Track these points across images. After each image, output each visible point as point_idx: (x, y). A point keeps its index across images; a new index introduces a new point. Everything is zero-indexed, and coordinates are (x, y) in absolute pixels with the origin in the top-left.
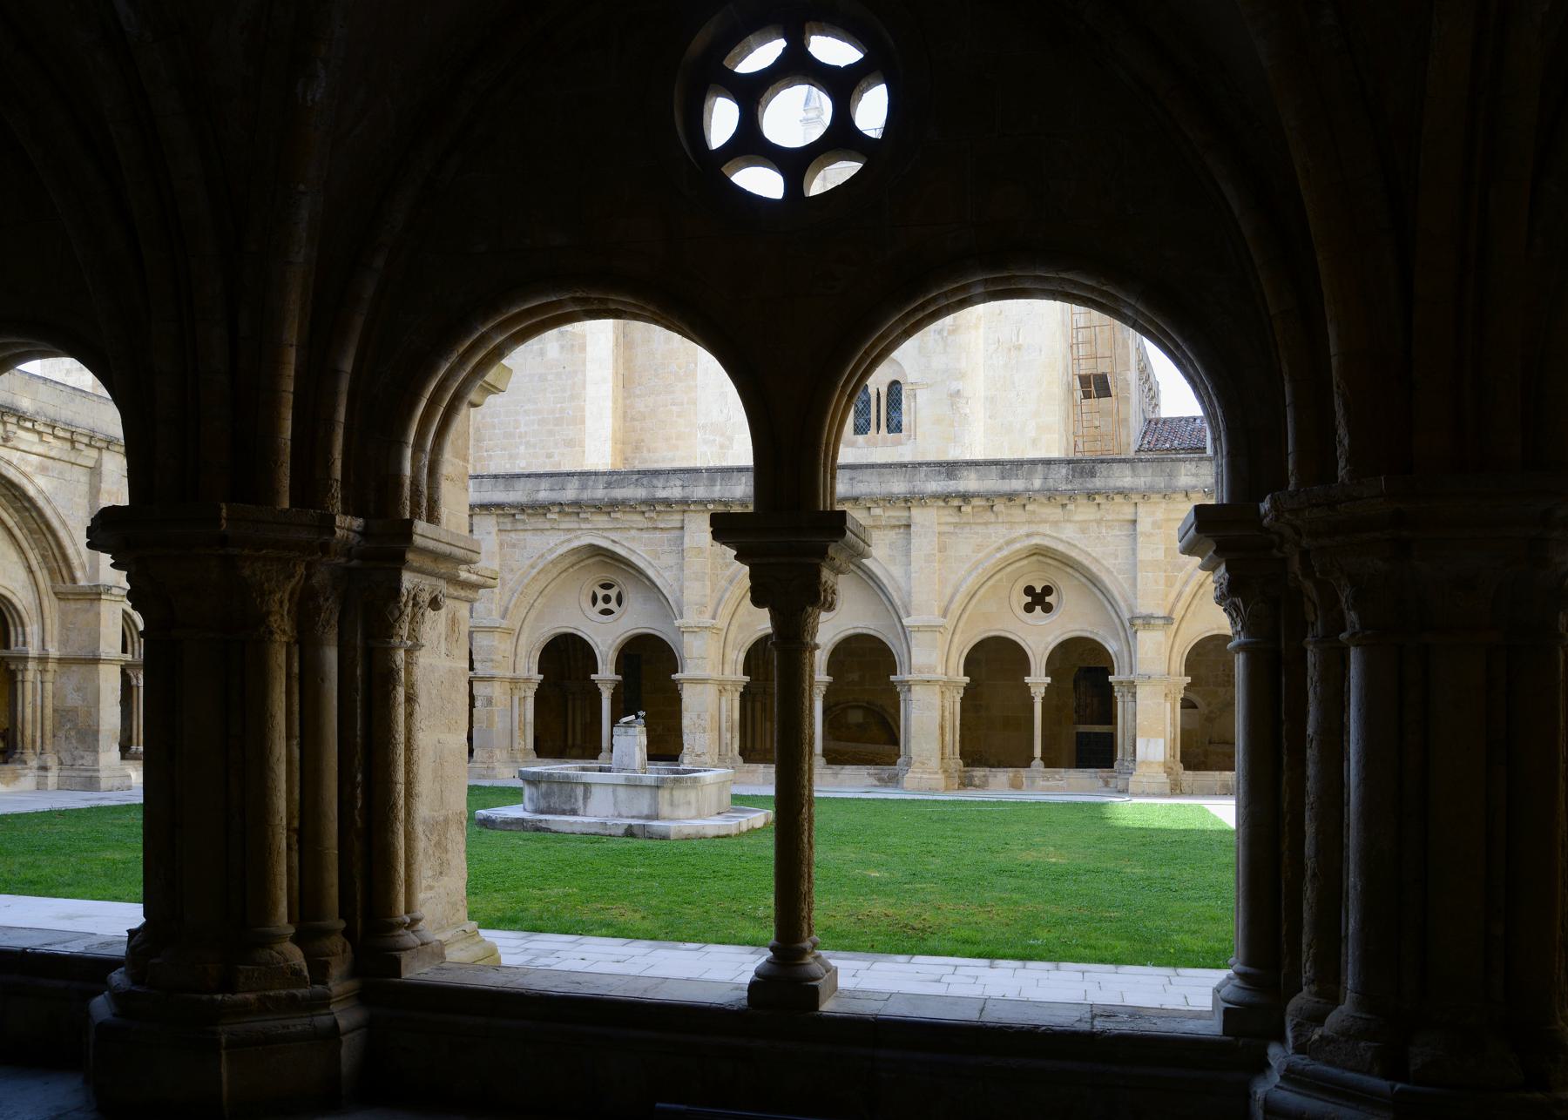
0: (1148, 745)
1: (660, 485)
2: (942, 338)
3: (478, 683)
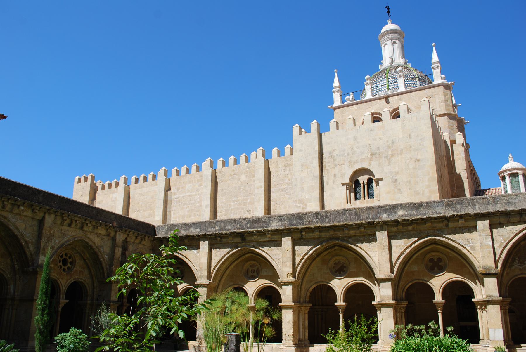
0: (495, 332)
2: (388, 159)
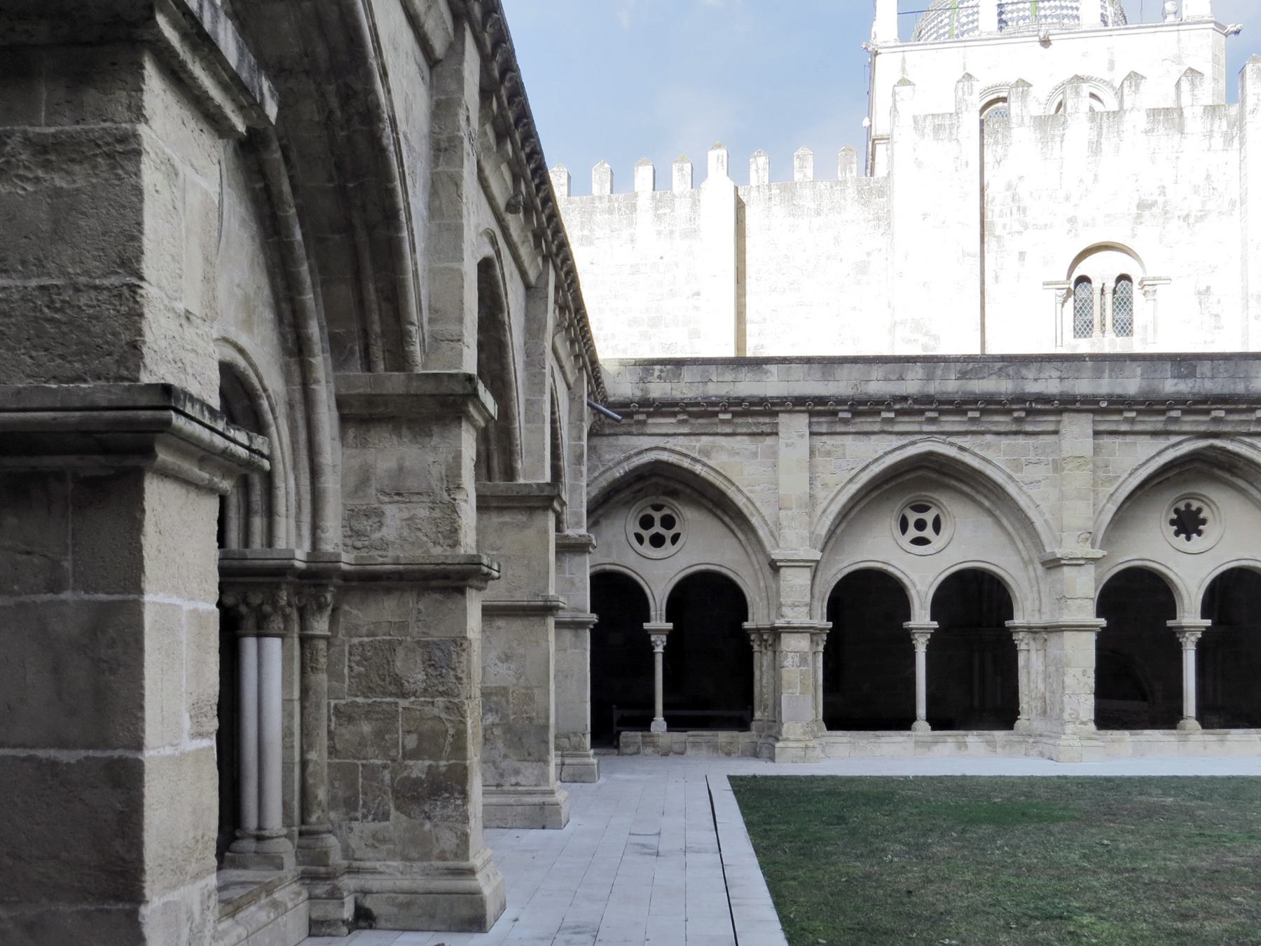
1: (1031, 376)
3: (787, 635)
